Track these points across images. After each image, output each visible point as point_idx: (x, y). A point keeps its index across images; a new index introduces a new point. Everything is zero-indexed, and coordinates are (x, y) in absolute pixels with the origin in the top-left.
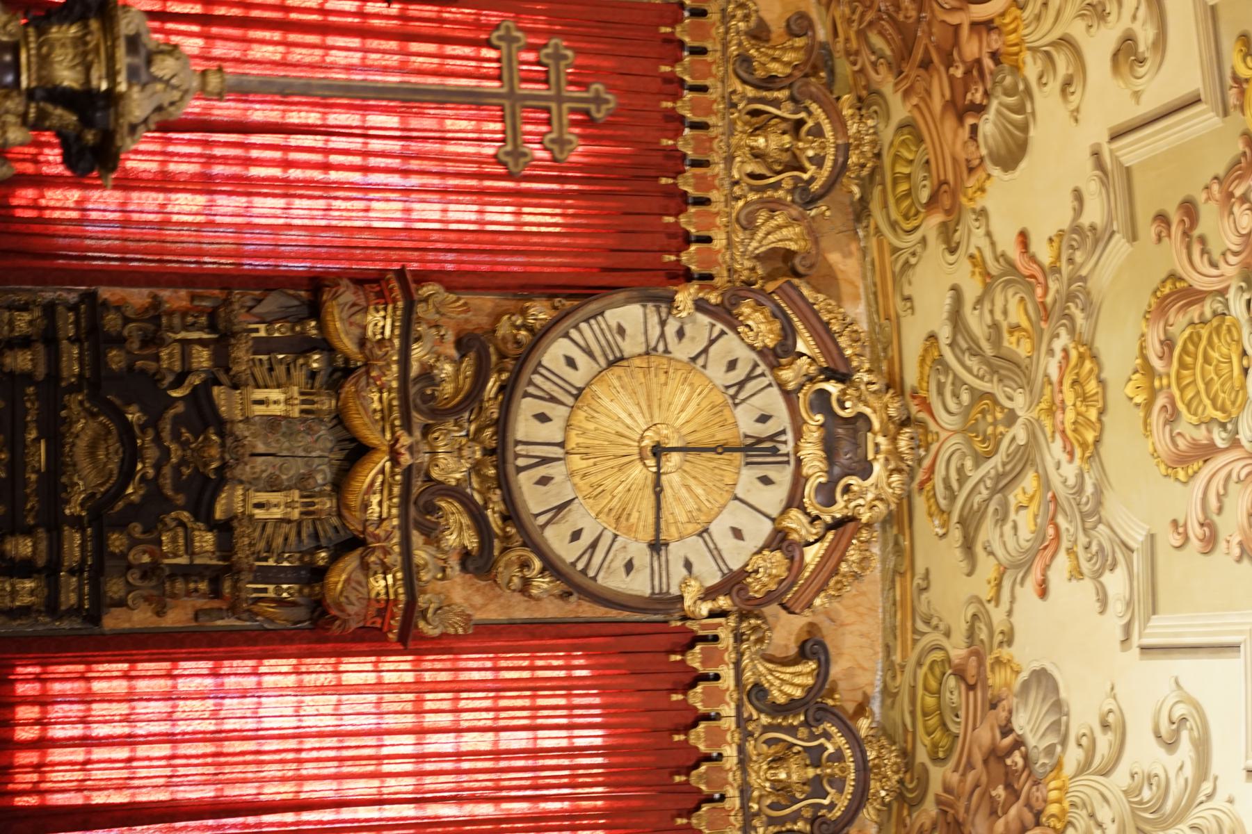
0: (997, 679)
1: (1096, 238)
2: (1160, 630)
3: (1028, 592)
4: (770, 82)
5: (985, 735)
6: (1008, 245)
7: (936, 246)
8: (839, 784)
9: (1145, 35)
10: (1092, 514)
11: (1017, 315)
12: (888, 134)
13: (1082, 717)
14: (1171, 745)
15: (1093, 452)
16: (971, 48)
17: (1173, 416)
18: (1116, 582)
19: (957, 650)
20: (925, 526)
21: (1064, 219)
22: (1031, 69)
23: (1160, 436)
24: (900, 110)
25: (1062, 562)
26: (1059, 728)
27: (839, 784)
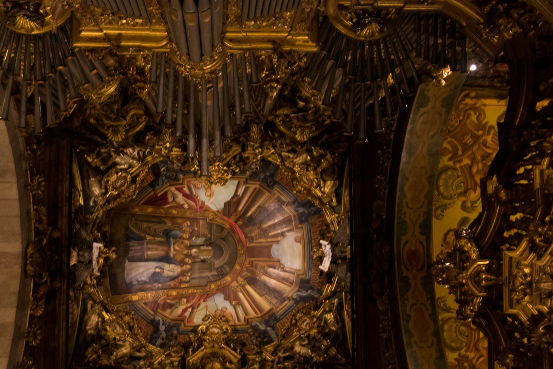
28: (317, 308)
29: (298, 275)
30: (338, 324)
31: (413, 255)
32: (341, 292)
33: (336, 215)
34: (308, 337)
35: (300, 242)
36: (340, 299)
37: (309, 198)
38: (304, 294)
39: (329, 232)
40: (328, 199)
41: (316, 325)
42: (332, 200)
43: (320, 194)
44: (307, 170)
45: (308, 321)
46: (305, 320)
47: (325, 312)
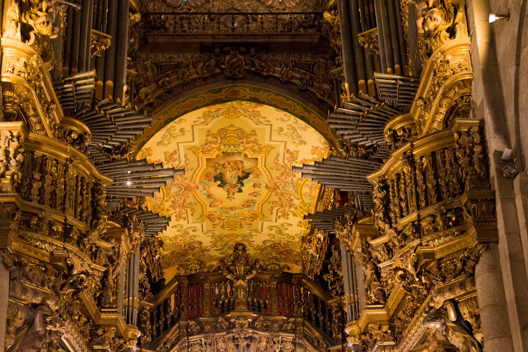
0: (263, 247)
1: (214, 234)
2: (260, 230)
3: (253, 243)
5: (269, 249)
6: (211, 244)
7: (209, 252)
8: (274, 267)
9: (193, 229)
10: (245, 236)
11: (220, 243)
12: (193, 258)
13: (269, 238)
14: (272, 229)
15: (238, 235)
17: (236, 227)
18: (254, 234)
19: (259, 252)
21: (210, 237)
22: (192, 241)
23: (238, 229)
25: (251, 239)
26: (270, 241)
27: (274, 267)
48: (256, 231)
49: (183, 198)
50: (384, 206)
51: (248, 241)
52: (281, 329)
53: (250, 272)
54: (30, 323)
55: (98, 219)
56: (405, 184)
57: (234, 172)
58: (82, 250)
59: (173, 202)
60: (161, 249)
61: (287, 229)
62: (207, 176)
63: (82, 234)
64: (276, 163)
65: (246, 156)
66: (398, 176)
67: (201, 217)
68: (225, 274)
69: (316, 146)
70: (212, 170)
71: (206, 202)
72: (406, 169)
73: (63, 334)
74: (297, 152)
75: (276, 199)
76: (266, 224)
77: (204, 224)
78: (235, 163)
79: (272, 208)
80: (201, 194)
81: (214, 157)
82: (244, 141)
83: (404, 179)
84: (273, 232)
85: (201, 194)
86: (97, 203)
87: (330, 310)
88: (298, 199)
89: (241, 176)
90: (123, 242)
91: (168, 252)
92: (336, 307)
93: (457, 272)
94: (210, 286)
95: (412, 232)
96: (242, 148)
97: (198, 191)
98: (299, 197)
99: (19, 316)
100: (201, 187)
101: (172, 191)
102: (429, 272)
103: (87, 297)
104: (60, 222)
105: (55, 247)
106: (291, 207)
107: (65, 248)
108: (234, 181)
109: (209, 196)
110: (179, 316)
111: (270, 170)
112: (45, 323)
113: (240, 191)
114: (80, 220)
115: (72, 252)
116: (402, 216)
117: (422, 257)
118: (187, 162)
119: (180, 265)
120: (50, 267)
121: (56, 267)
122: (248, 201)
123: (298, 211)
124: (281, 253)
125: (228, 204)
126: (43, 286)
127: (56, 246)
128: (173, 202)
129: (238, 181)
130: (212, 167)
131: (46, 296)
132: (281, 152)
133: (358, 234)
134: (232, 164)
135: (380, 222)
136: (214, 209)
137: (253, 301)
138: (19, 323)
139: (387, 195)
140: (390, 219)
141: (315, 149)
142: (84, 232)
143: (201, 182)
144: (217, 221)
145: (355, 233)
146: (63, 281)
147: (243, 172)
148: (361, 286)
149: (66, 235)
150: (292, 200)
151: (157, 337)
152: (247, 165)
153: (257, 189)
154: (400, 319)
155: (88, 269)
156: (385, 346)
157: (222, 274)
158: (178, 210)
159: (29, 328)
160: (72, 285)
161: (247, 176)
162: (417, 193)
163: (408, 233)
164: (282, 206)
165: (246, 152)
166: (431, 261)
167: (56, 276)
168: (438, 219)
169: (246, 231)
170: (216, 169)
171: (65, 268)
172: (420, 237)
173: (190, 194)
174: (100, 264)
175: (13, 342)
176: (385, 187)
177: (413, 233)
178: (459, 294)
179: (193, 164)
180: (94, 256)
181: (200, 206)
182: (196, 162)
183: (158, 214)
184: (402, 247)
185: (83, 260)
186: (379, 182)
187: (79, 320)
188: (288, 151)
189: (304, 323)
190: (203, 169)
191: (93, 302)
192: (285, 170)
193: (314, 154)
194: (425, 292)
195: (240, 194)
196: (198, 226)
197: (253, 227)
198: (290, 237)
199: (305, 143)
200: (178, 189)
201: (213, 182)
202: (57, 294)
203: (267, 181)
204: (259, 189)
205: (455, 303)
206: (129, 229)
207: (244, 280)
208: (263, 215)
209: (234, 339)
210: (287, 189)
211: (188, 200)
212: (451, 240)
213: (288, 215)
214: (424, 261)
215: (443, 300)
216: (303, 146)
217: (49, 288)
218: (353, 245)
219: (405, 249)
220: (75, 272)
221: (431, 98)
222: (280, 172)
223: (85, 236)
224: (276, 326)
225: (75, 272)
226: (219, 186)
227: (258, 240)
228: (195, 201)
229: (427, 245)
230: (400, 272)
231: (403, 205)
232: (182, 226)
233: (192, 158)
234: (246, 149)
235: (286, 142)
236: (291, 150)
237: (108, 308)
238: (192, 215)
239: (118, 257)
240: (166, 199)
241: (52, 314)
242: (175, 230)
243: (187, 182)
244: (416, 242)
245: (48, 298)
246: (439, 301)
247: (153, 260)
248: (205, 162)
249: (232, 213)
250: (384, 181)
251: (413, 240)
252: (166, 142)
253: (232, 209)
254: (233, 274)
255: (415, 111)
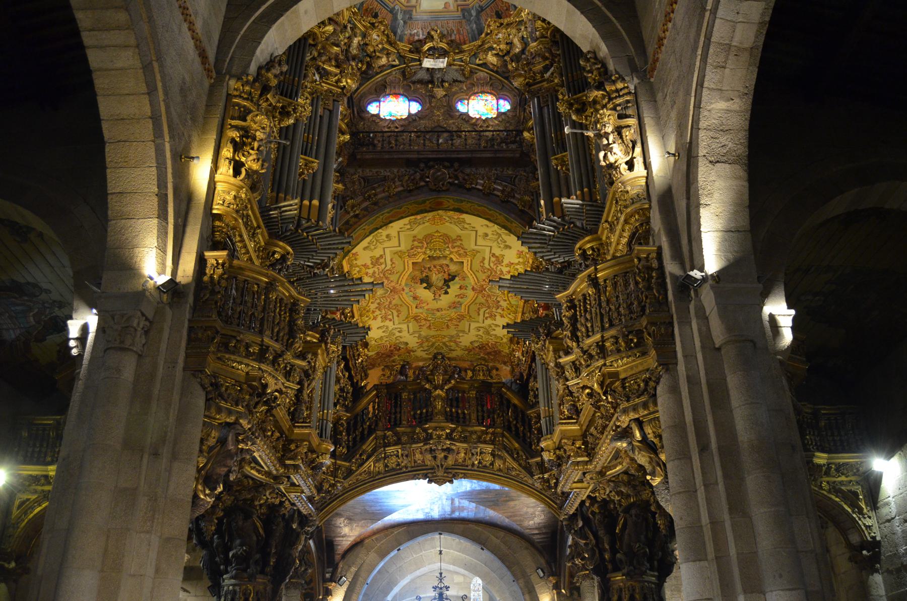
0: (471, 348)
1: (420, 335)
2: (467, 330)
4: (391, 374)
5: (477, 349)
6: (417, 345)
10: (452, 337)
13: (476, 339)
16: (392, 348)
18: (461, 335)
20: (450, 355)
24: (396, 357)
28: (390, 43)
29: (415, 7)
30: (379, 67)
31: (441, 204)
32: (405, 63)
33: (468, 59)
34: (366, 44)
35: (445, 8)
36: (399, 65)
37: (483, 35)
38: (400, 16)
39: (454, 49)
40: (481, 58)
41: (377, 48)
42: (480, 60)
43: (486, 46)
44: (507, 44)
45: (379, 39)
46: (378, 36)
47: (388, 58)
48: (463, 332)
49: (389, 300)
50: (571, 325)
51: (455, 342)
52: (480, 440)
53: (448, 381)
54: (222, 441)
55: (294, 338)
56: (590, 304)
57: (440, 275)
58: (277, 370)
59: (379, 304)
60: (366, 350)
61: (494, 330)
62: (413, 278)
63: (277, 354)
64: (482, 267)
65: (451, 260)
66: (584, 295)
67: (407, 318)
68: (424, 383)
69: (521, 250)
70: (417, 273)
71: (411, 304)
72: (591, 291)
73: (254, 452)
74: (503, 256)
75: (483, 301)
76: (474, 325)
77: (410, 325)
78: (441, 266)
79: (479, 309)
80: (407, 297)
81: (420, 260)
82: (450, 246)
83: (590, 300)
84: (480, 333)
85: (407, 297)
86: (294, 322)
87: (530, 420)
88: (505, 300)
89: (447, 278)
90: (320, 357)
91: (373, 353)
92: (535, 417)
93: (640, 393)
94: (408, 395)
95: (597, 353)
96: (448, 253)
97: (404, 293)
98: (506, 298)
99: (213, 435)
100: (407, 290)
101: (378, 293)
102: (615, 392)
103: (281, 414)
104: (256, 343)
105: (250, 368)
106: (498, 308)
107: (260, 369)
108: (441, 284)
109: (415, 298)
110: (377, 425)
111: (476, 273)
112: (238, 442)
113: (446, 293)
114: (277, 340)
115: (267, 371)
116: (588, 336)
117: (607, 377)
118: (393, 266)
119: (385, 366)
120: (245, 386)
121: (250, 386)
122: (454, 303)
123: (505, 313)
124: (489, 354)
125: (434, 305)
126: (237, 405)
127: (252, 366)
128: (379, 304)
129: (445, 283)
130: (418, 270)
131: (240, 415)
132: (487, 256)
133: (551, 348)
134: (438, 267)
135: (568, 341)
136: (420, 310)
137: (451, 411)
138: (212, 442)
139: (575, 315)
140: (577, 337)
141: (520, 254)
142: (279, 352)
143: (406, 285)
144: (423, 322)
145: (549, 348)
146: (256, 399)
147: (449, 275)
148: (555, 401)
149: (261, 357)
150: (499, 302)
151: (353, 448)
152: (453, 268)
153: (463, 291)
154: (592, 435)
155: (282, 387)
156: (579, 462)
157: (420, 383)
158: (384, 312)
159: (221, 447)
160: (266, 403)
161: (453, 278)
162: (601, 313)
163: (594, 353)
164: (489, 307)
165: (452, 256)
166: (616, 381)
167: (250, 395)
168: (620, 340)
169: (452, 331)
170: (422, 272)
171: (260, 387)
172: (604, 358)
173: (396, 296)
174: (293, 382)
175: (205, 461)
176: (572, 305)
177: (598, 354)
178: (642, 414)
179: (399, 266)
180: (288, 375)
181: (406, 308)
182: (402, 266)
183: (357, 325)
184: (588, 366)
185: (277, 379)
186: (567, 302)
187: (272, 435)
188: (494, 255)
189: (503, 433)
190: (409, 273)
191: (287, 417)
192: (491, 273)
193: (519, 257)
194: (612, 411)
195: (446, 296)
196: (404, 327)
197: (460, 328)
198: (498, 337)
199: (510, 248)
200: (383, 292)
201: (419, 284)
202: (251, 412)
203: (473, 283)
204: (465, 291)
205: (640, 423)
206: (326, 344)
207: (442, 389)
208: (470, 317)
209: (431, 451)
210: (494, 291)
211: (394, 302)
212: (634, 361)
213: (495, 316)
214: (608, 381)
215: (627, 420)
216: (508, 250)
217: (243, 407)
218: (547, 358)
219: (591, 369)
220: (269, 391)
221: (615, 222)
222: (486, 274)
223: (280, 356)
224: (474, 437)
225: (269, 391)
226: (425, 288)
227: (466, 340)
228: (401, 303)
229: (611, 366)
230: (587, 391)
231: (589, 325)
232: (387, 327)
233: (398, 261)
234: (451, 253)
235: (491, 247)
236: (497, 255)
237: (302, 423)
238: (398, 316)
239: (314, 371)
240: (371, 300)
241: (245, 432)
242: (381, 331)
243: (393, 284)
244: (601, 362)
245: (241, 417)
246: (624, 421)
247: (356, 363)
248: (411, 265)
249: (438, 314)
250: (571, 301)
251: (597, 360)
252: (373, 247)
253: (438, 310)
254: (431, 383)
255: (602, 233)
